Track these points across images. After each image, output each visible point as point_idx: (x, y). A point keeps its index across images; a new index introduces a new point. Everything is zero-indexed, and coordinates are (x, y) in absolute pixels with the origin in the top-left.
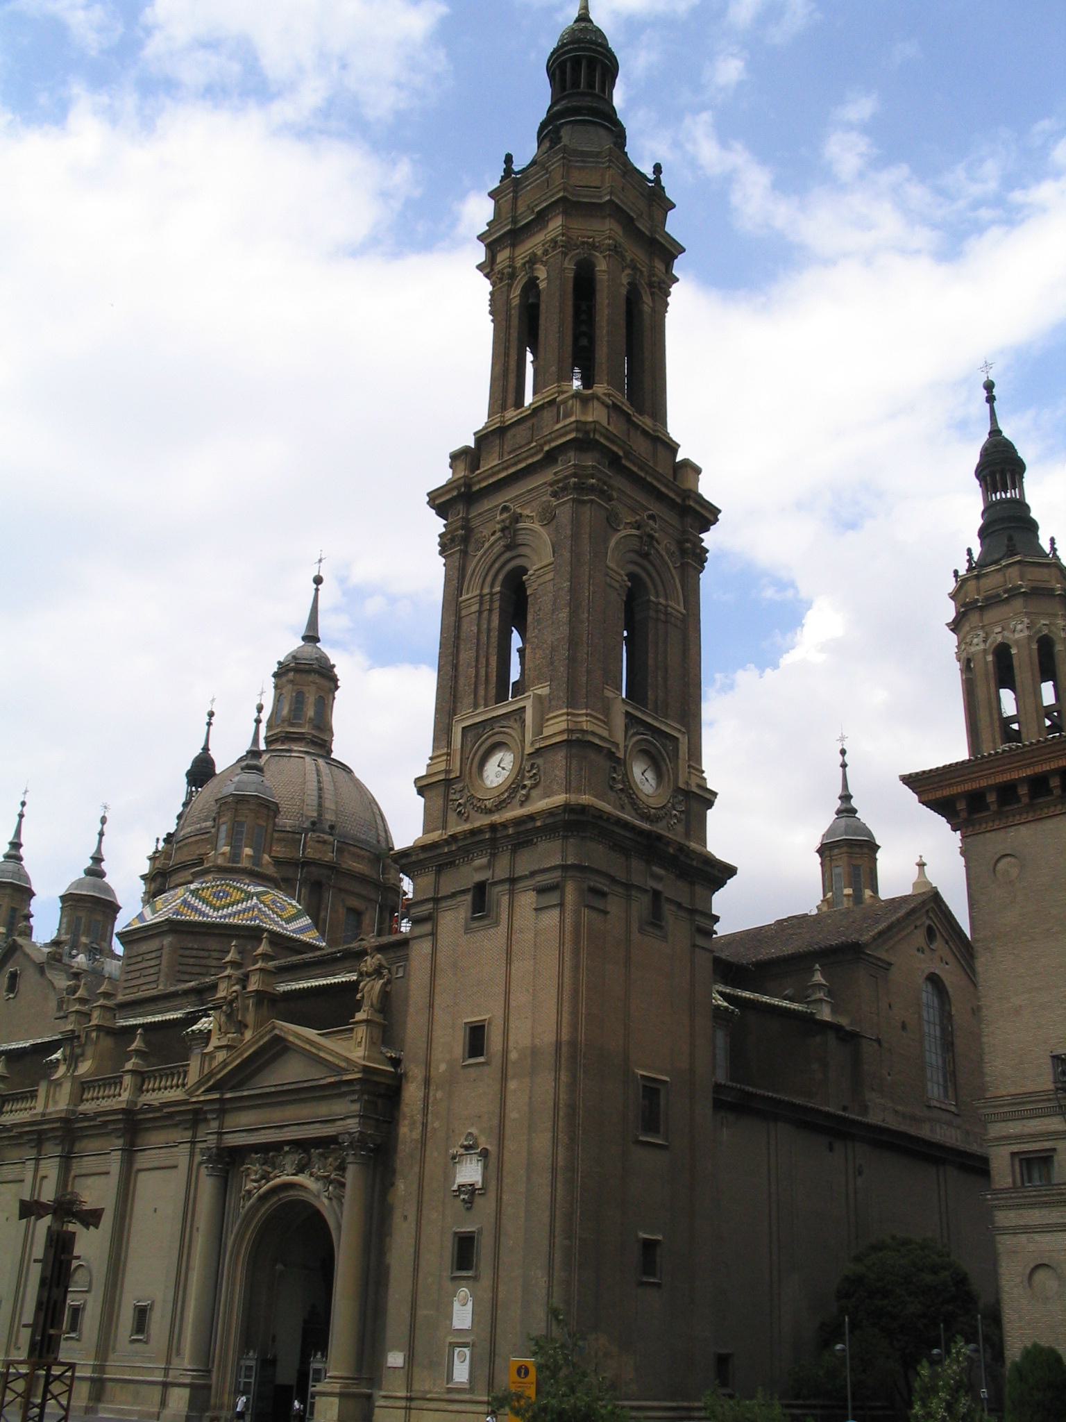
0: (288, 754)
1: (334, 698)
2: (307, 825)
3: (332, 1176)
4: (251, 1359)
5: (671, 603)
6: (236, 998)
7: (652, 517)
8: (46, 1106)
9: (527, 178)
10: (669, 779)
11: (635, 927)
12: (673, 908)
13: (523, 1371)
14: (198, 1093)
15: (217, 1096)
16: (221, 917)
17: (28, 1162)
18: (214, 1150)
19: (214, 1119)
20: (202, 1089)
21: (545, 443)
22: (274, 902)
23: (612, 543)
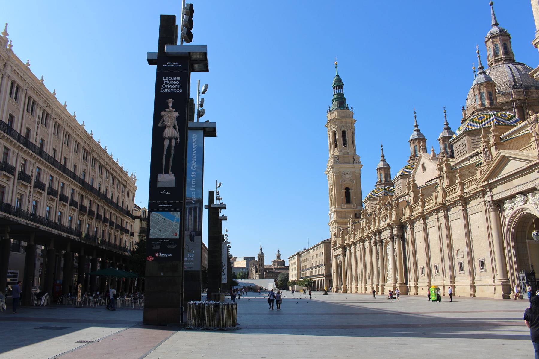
0: (497, 67)
1: (510, 42)
4: (523, 274)
8: (436, 201)
15: (486, 183)
16: (482, 126)
17: (435, 220)
18: (491, 202)
19: (488, 191)
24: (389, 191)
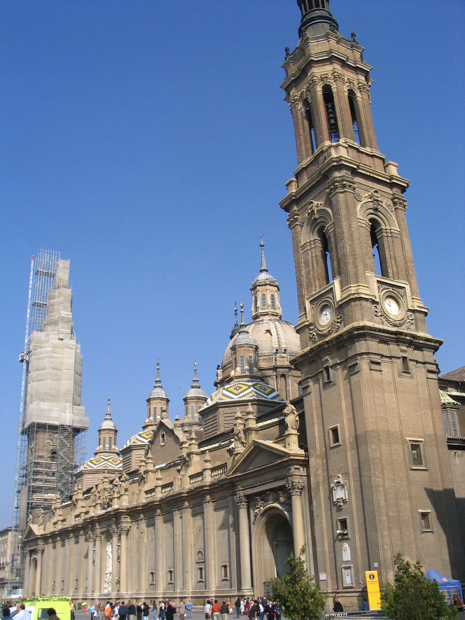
2: (274, 351)
3: (287, 502)
5: (392, 228)
6: (240, 432)
7: (376, 192)
9: (296, 55)
10: (404, 306)
11: (396, 374)
12: (414, 363)
13: (372, 576)
14: (230, 474)
16: (239, 398)
20: (231, 473)
21: (321, 170)
22: (261, 387)
23: (358, 208)
24: (111, 463)
